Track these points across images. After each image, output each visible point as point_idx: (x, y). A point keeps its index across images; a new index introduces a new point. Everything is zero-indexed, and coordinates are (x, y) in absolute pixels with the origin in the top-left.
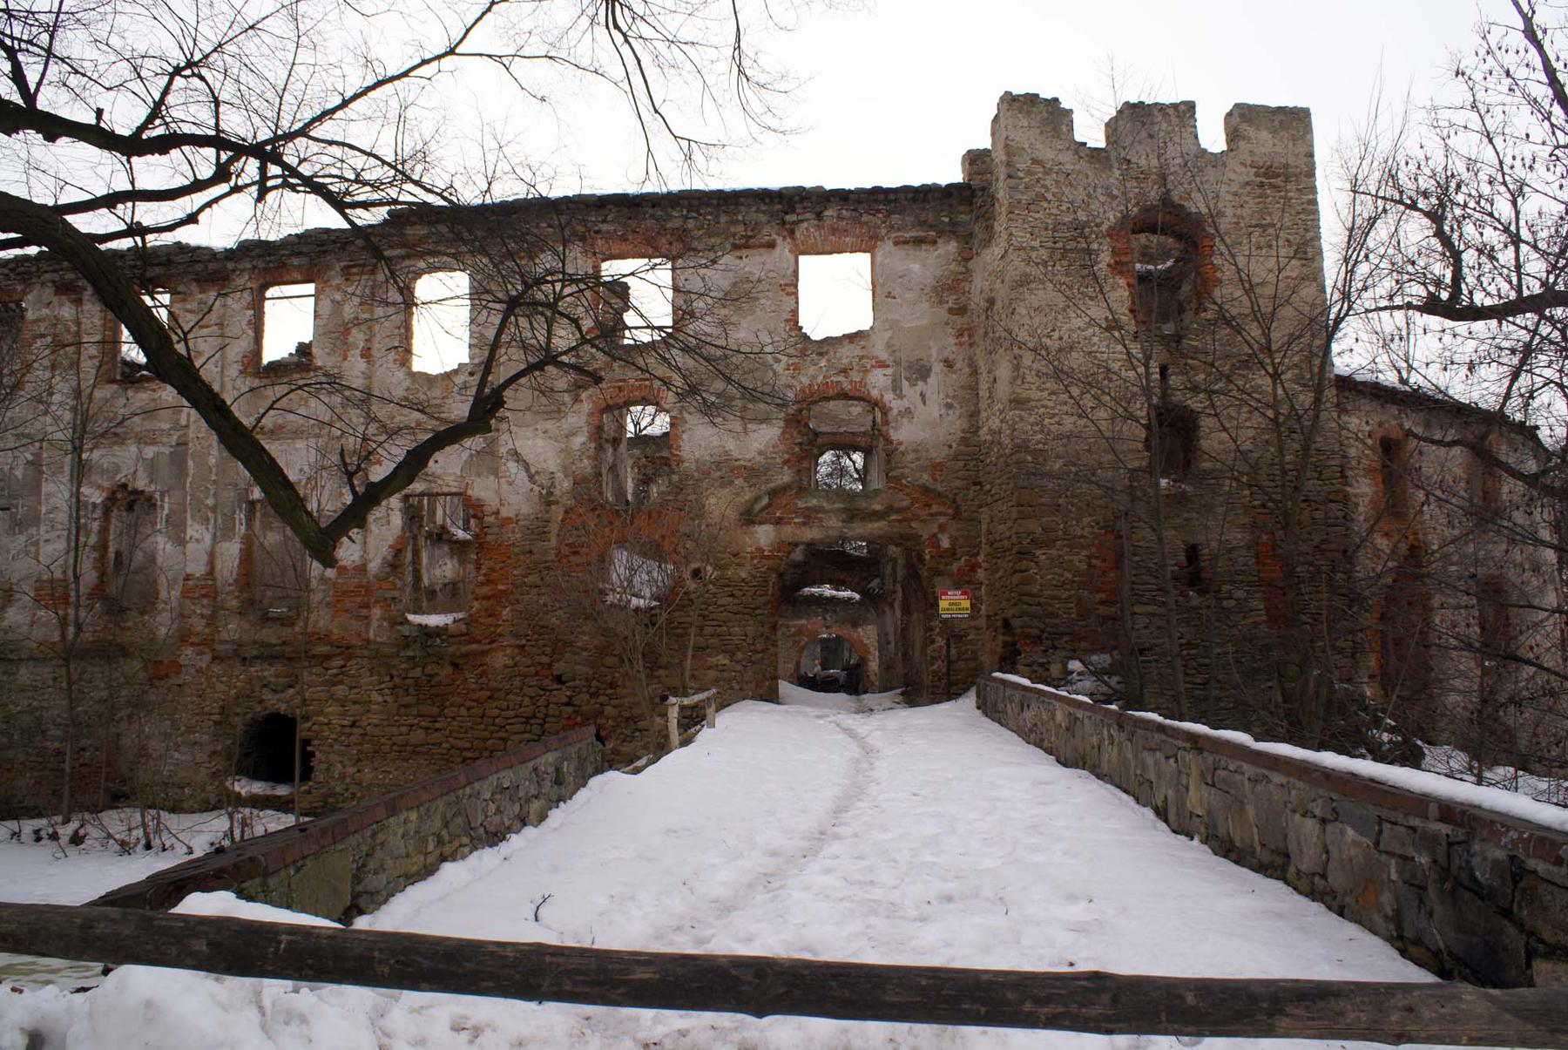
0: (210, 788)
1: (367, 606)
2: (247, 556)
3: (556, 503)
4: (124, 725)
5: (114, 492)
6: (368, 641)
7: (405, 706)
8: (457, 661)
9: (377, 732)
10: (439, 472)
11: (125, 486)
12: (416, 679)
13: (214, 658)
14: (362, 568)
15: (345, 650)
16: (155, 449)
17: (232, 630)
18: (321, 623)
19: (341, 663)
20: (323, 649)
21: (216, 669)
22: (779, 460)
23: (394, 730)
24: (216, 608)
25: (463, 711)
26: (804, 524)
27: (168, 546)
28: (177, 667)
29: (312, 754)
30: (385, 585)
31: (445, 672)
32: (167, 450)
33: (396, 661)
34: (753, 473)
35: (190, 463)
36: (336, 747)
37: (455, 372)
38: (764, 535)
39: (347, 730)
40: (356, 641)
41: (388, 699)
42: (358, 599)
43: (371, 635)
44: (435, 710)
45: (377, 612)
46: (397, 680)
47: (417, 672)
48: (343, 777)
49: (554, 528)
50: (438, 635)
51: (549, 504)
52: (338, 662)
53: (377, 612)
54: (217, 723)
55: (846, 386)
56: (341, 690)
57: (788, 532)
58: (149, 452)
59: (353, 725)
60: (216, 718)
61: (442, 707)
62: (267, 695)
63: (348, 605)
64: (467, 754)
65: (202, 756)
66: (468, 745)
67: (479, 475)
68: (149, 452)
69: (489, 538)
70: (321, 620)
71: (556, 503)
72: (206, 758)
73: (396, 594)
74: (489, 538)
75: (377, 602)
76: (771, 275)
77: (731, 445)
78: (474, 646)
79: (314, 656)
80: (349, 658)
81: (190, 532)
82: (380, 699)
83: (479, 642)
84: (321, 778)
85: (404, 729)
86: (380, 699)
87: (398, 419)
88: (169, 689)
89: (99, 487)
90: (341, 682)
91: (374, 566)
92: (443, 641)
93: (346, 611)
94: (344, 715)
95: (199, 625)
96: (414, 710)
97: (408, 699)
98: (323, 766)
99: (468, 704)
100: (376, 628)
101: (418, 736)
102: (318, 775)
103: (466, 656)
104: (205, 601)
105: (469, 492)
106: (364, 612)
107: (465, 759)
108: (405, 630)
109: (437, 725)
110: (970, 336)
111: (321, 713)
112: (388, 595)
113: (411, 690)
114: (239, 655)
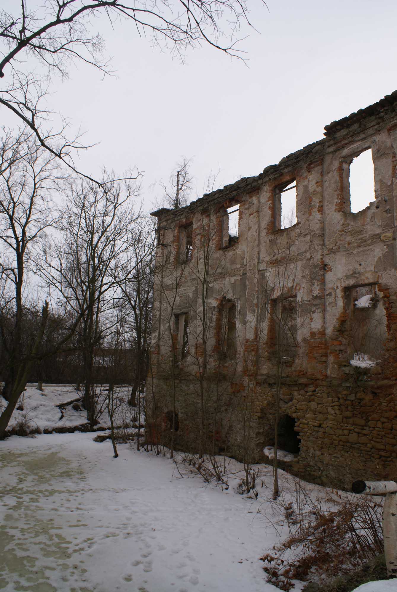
0: (256, 451)
1: (326, 355)
2: (272, 329)
4: (223, 414)
5: (222, 301)
6: (326, 376)
7: (347, 418)
8: (376, 391)
9: (331, 432)
10: (362, 270)
12: (352, 401)
13: (257, 383)
14: (323, 333)
15: (314, 381)
16: (235, 278)
17: (265, 369)
18: (304, 366)
20: (303, 380)
21: (258, 389)
23: (340, 432)
24: (258, 356)
25: (379, 425)
27: (240, 326)
28: (243, 387)
29: (299, 440)
30: (335, 343)
31: (368, 397)
32: (239, 278)
33: (341, 389)
35: (247, 283)
36: (311, 438)
37: (368, 208)
40: (319, 376)
41: (337, 412)
42: (320, 351)
43: (329, 373)
44: (363, 422)
45: (331, 359)
46: (341, 401)
47: (352, 397)
48: (314, 456)
50: (365, 374)
52: (311, 388)
53: (331, 359)
54: (259, 418)
56: (313, 405)
58: (233, 280)
60: (259, 414)
61: (367, 420)
62: (282, 404)
63: (315, 355)
64: (383, 453)
65: (253, 435)
66: (382, 447)
67: (385, 269)
68: (233, 280)
70: (301, 363)
72: (254, 436)
73: (342, 348)
75: (331, 353)
78: (386, 382)
79: (300, 384)
80: (317, 386)
81: (248, 318)
82: (333, 412)
83: (388, 379)
84: (303, 455)
85: (346, 432)
86: (333, 412)
87: (339, 243)
91: (329, 331)
92: (368, 377)
93: (315, 358)
94: (315, 419)
95: (250, 366)
96: (351, 421)
97: (348, 414)
98: (305, 448)
99: (383, 420)
100: (331, 370)
101: (353, 437)
102: (302, 453)
103: (378, 388)
105: (380, 281)
106: (324, 359)
107: (381, 457)
108: (346, 370)
109: (364, 432)
111: (304, 417)
112: (338, 348)
113: (349, 408)
114: (268, 382)
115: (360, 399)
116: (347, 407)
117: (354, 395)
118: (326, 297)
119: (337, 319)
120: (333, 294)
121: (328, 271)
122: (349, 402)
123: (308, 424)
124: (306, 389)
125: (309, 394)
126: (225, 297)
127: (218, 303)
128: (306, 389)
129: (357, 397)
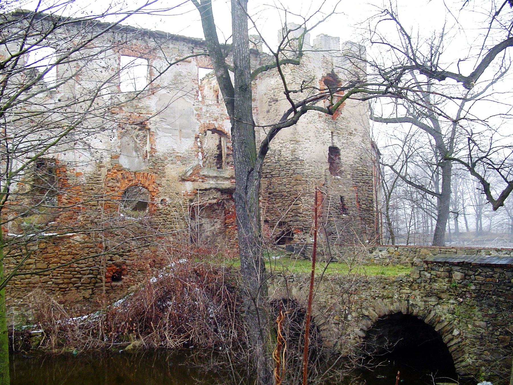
3: (104, 167)
22: (193, 155)
34: (184, 160)
38: (189, 186)
49: (102, 177)
51: (100, 167)
55: (217, 126)
64: (62, 286)
66: (61, 282)
69: (69, 181)
71: (104, 167)
74: (69, 181)
77: (175, 147)
82: (15, 261)
85: (28, 276)
107: (61, 288)
110: (257, 110)
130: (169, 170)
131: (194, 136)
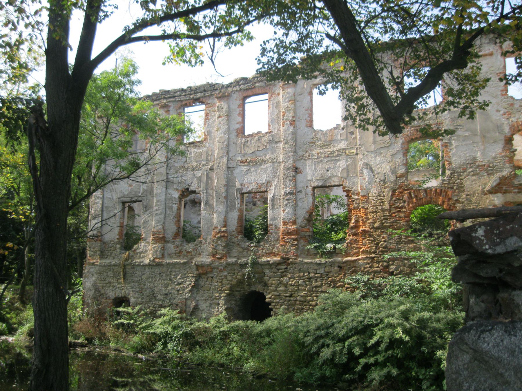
5: (183, 192)
11: (188, 189)
19: (285, 267)
26: (519, 192)
37: (335, 128)
39: (288, 298)
57: (510, 197)
59: (291, 296)
75: (301, 238)
76: (492, 69)
88: (207, 279)
89: (177, 190)
90: (285, 276)
104: (223, 239)
113: (318, 280)
115: (328, 272)
116: (317, 279)
117: (323, 269)
118: (297, 194)
119: (307, 212)
120: (304, 191)
121: (299, 173)
122: (319, 275)
123: (279, 296)
124: (278, 267)
125: (280, 271)
126: (188, 189)
127: (179, 193)
128: (278, 267)
129: (326, 271)
130: (468, 183)
131: (502, 138)
